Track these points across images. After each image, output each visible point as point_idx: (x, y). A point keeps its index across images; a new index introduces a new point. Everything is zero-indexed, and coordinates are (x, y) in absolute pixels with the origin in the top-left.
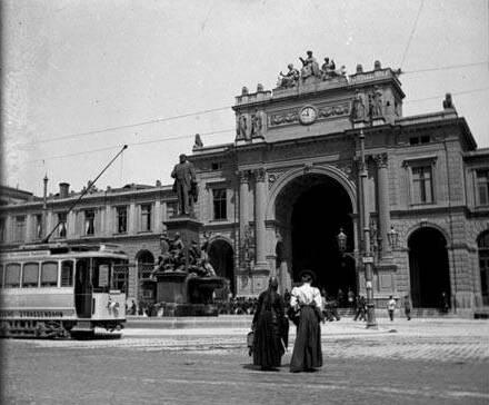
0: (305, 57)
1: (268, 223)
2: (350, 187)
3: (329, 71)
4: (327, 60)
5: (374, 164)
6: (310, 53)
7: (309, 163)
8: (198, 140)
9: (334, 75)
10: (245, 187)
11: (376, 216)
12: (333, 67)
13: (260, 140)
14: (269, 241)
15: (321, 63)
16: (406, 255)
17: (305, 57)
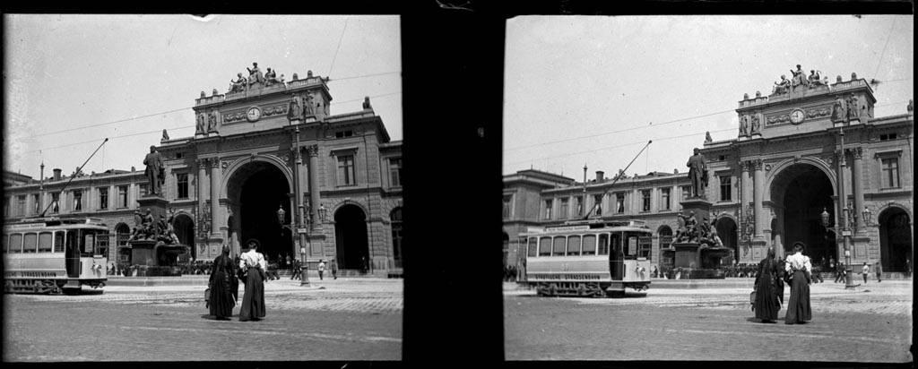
0: (252, 68)
1: (221, 201)
2: (288, 172)
3: (271, 78)
4: (269, 70)
5: (307, 153)
6: (255, 64)
7: (254, 152)
8: (165, 134)
9: (275, 82)
10: (203, 172)
11: (309, 195)
12: (274, 75)
13: (215, 135)
14: (222, 215)
15: (265, 72)
16: (333, 227)
17: (252, 68)
